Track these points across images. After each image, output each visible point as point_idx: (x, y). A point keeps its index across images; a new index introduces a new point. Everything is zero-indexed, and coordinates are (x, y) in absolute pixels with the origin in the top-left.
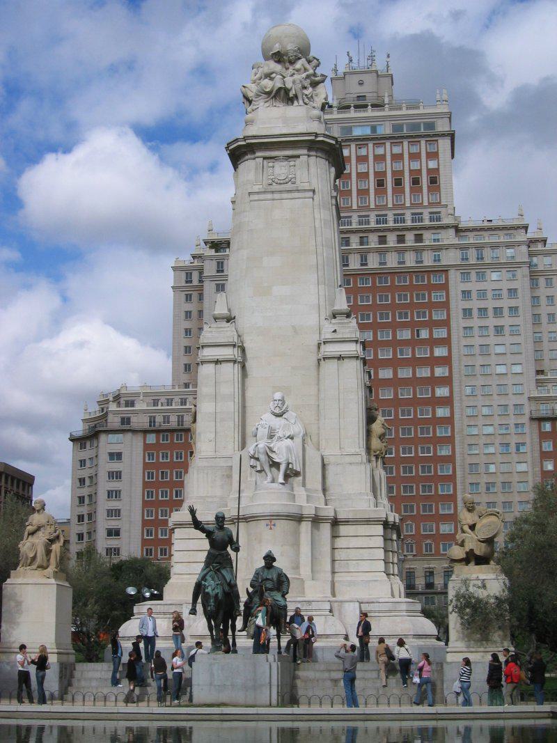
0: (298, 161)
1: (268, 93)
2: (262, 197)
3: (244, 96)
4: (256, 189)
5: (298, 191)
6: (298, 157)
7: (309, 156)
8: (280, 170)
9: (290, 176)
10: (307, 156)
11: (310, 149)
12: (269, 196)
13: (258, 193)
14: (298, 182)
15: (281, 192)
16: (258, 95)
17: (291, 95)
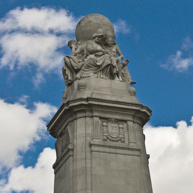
0: (125, 125)
1: (99, 66)
2: (101, 149)
3: (66, 63)
4: (96, 141)
5: (129, 149)
6: (126, 121)
7: (134, 122)
8: (113, 129)
9: (120, 136)
10: (132, 122)
11: (134, 117)
12: (107, 150)
13: (99, 146)
14: (127, 142)
15: (116, 148)
16: (88, 66)
17: (115, 72)
